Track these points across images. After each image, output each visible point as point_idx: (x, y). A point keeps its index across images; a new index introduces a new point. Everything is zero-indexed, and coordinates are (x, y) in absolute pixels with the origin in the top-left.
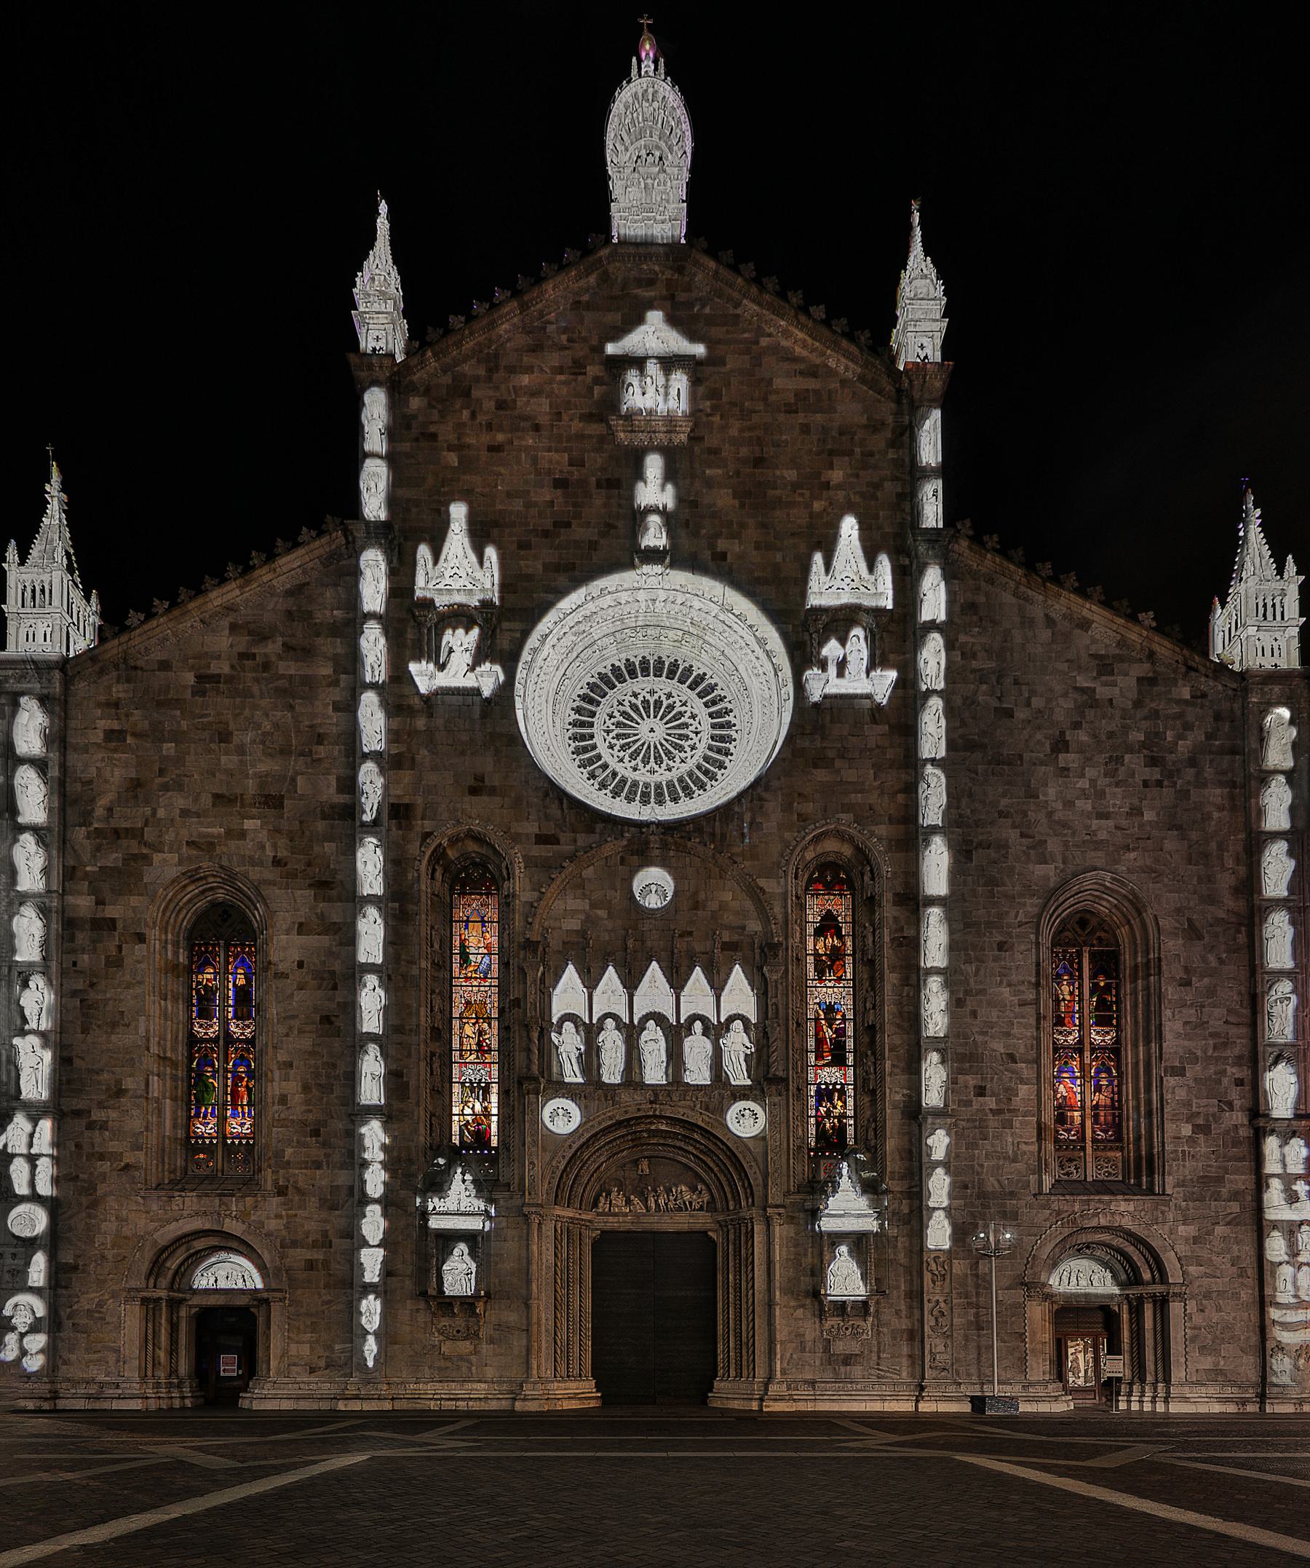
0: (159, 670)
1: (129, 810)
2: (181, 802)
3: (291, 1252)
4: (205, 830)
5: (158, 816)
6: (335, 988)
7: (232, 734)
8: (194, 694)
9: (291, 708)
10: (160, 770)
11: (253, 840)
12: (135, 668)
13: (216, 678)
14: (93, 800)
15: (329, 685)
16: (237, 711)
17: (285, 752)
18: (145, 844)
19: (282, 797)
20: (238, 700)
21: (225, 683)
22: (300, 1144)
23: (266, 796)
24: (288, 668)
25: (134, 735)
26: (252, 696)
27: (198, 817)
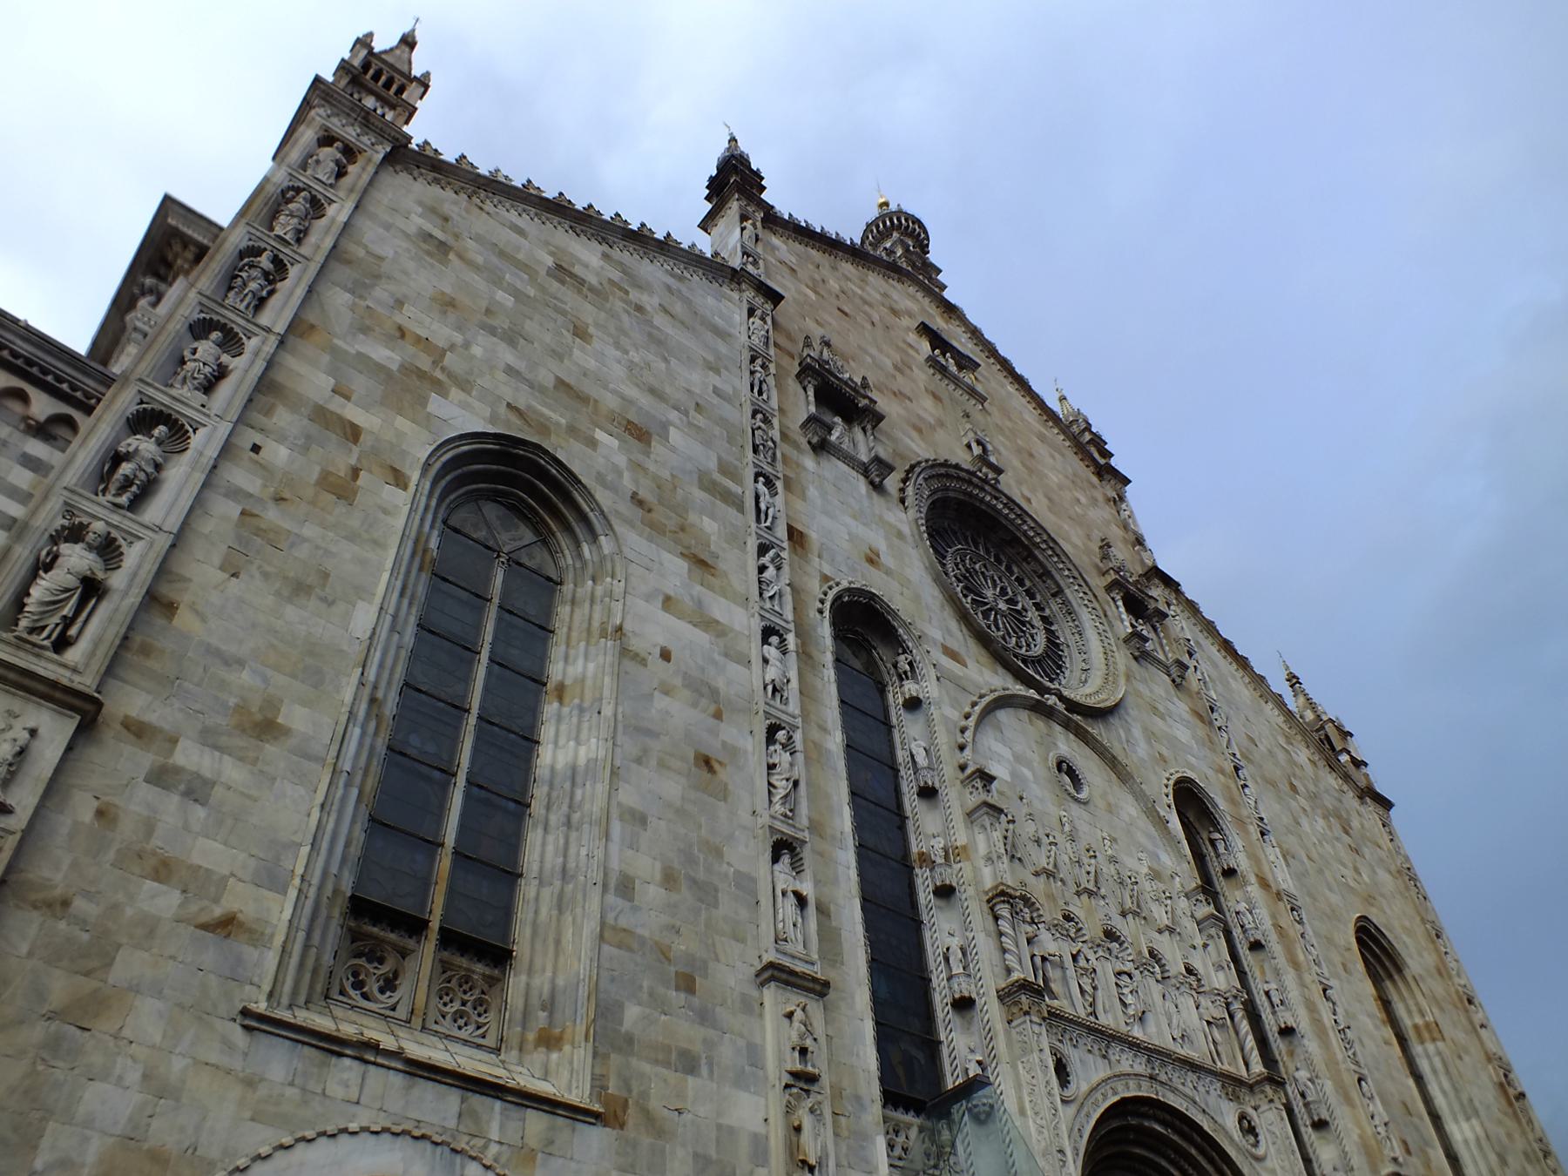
0: (510, 228)
1: (429, 320)
2: (507, 356)
4: (540, 407)
6: (718, 716)
7: (592, 337)
8: (548, 274)
10: (488, 312)
12: (481, 209)
13: (582, 282)
14: (378, 277)
15: (711, 369)
18: (443, 369)
20: (603, 315)
21: (589, 289)
23: (629, 422)
25: (460, 257)
27: (532, 386)
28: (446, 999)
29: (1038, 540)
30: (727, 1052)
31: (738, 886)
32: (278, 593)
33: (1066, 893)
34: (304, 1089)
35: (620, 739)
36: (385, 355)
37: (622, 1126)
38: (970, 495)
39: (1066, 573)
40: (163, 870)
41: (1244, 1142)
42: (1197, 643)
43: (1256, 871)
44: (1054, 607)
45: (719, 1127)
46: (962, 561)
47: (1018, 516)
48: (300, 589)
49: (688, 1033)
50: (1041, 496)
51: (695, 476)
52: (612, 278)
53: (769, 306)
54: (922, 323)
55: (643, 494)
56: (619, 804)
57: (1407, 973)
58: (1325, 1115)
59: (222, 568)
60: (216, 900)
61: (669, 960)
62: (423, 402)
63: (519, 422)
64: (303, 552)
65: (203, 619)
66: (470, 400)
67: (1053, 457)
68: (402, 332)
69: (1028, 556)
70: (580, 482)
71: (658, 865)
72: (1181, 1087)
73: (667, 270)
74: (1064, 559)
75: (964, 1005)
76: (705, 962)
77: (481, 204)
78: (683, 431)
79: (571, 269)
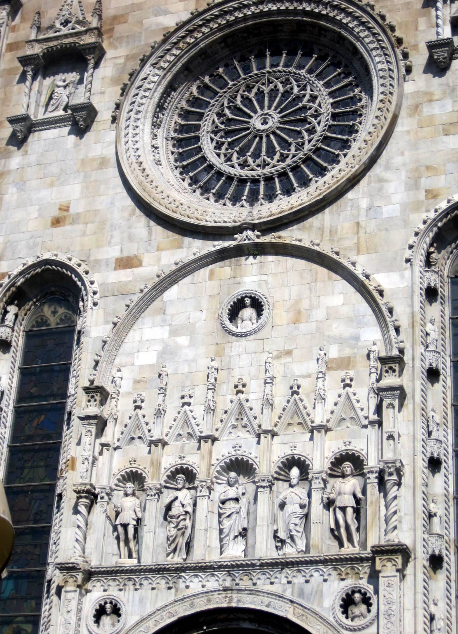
38: (229, 24)
46: (230, 101)
72: (268, 588)
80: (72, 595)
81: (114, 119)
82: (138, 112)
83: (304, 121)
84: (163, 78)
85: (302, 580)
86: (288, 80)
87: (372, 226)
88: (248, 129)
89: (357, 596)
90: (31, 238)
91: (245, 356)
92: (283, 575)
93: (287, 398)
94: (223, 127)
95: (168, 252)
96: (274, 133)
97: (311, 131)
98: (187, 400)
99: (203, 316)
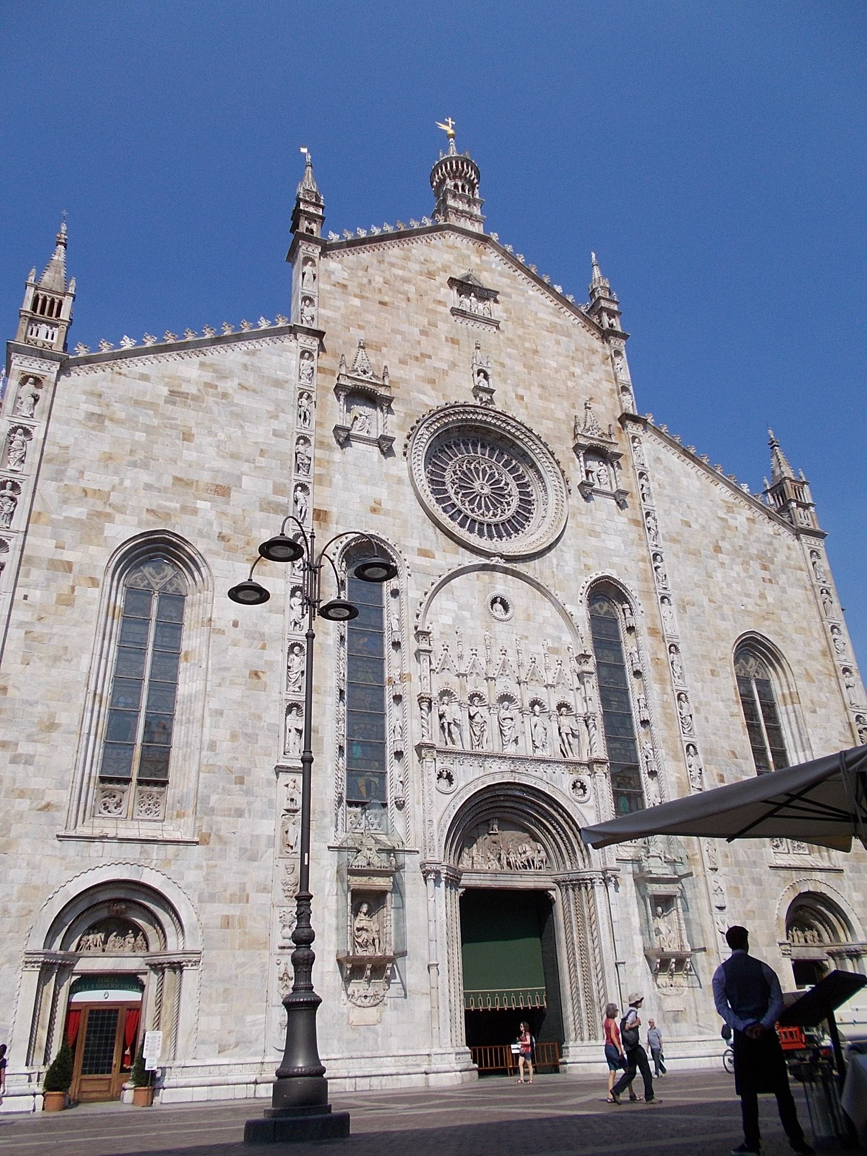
0: (139, 379)
1: (99, 476)
2: (145, 477)
3: (208, 907)
4: (164, 503)
5: (125, 485)
6: (263, 647)
7: (193, 435)
8: (166, 402)
9: (242, 427)
10: (131, 451)
11: (203, 517)
12: (120, 374)
13: (185, 395)
14: (67, 462)
15: (271, 418)
16: (199, 421)
17: (234, 456)
18: (110, 505)
19: (229, 488)
20: (201, 413)
21: (192, 399)
22: (228, 792)
23: (217, 486)
24: (241, 399)
25: (111, 420)
26: (212, 413)
27: (160, 492)
28: (142, 805)
29: (518, 433)
30: (258, 805)
31: (269, 730)
32: (47, 665)
33: (477, 681)
34: (82, 856)
35: (209, 679)
36: (78, 511)
37: (208, 844)
38: (467, 420)
39: (538, 451)
40: (22, 794)
41: (574, 795)
42: (658, 460)
43: (650, 625)
44: (530, 477)
45: (252, 836)
46: (460, 467)
47: (503, 421)
48: (56, 659)
49: (238, 800)
50: (536, 390)
51: (258, 504)
52: (206, 381)
53: (316, 342)
54: (451, 278)
55: (226, 531)
56: (210, 709)
57: (783, 662)
58: (654, 768)
59: (22, 663)
60: (43, 799)
61: (232, 772)
62: (101, 530)
63: (153, 519)
64: (55, 641)
65: (19, 690)
66: (126, 517)
67: (558, 343)
68: (85, 491)
69: (513, 445)
70: (187, 542)
71: (228, 731)
72: (534, 773)
73: (244, 351)
74: (537, 442)
75: (399, 755)
76: (250, 770)
77: (119, 371)
78: (251, 476)
79: (179, 390)
80: (429, 764)
81: (405, 454)
82: (418, 455)
83: (503, 496)
84: (430, 438)
85: (551, 771)
86: (491, 466)
87: (561, 575)
88: (472, 489)
89: (579, 784)
90: (357, 516)
91: (503, 633)
92: (541, 767)
93: (530, 665)
94: (457, 481)
95: (451, 555)
96: (488, 497)
97: (508, 504)
98: (474, 652)
99: (477, 601)
